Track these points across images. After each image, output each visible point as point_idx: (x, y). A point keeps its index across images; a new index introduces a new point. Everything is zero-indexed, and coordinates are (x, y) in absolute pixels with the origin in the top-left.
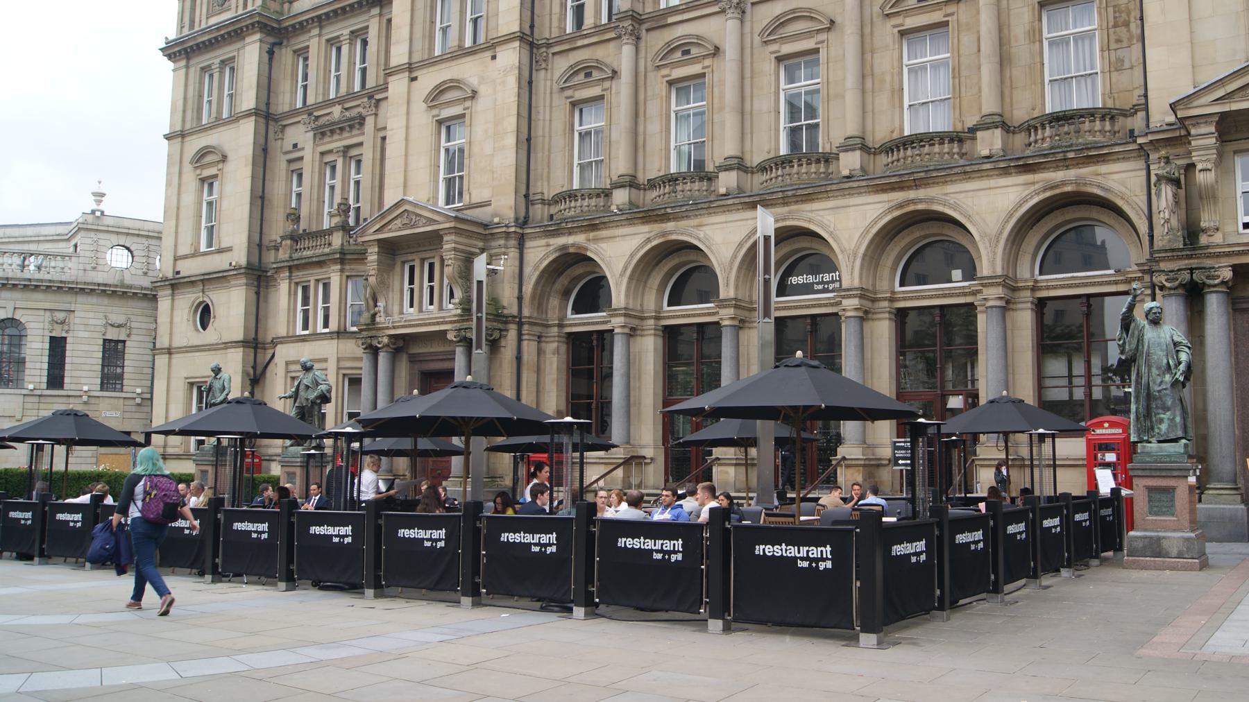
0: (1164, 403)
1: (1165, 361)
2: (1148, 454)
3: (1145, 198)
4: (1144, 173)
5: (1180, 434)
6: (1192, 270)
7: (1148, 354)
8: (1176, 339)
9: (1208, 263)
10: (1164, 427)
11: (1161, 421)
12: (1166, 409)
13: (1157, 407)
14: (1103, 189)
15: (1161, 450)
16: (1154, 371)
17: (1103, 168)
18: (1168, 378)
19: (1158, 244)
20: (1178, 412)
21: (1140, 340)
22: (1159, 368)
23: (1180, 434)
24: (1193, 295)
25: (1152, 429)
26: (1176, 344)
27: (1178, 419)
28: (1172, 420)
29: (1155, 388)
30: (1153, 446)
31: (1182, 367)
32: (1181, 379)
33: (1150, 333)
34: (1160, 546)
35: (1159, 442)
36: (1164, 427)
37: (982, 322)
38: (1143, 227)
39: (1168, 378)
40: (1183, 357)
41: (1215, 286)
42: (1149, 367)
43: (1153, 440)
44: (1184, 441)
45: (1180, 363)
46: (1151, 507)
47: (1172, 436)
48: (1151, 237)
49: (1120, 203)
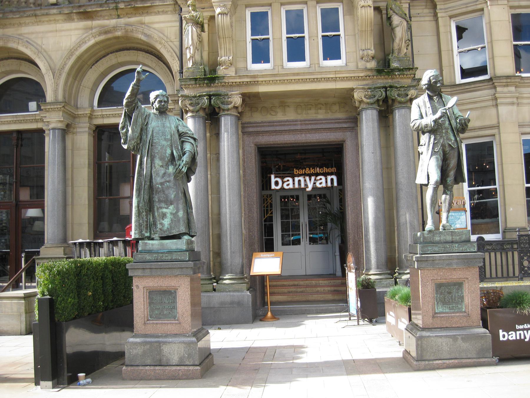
0: (167, 196)
1: (169, 151)
2: (150, 252)
3: (178, 44)
4: (178, 24)
5: (183, 229)
6: (210, 96)
7: (151, 144)
8: (181, 129)
9: (222, 90)
10: (166, 222)
11: (164, 216)
12: (169, 202)
13: (160, 201)
14: (146, 35)
15: (162, 245)
16: (158, 162)
17: (147, 19)
18: (171, 169)
19: (185, 75)
20: (181, 206)
21: (143, 129)
22: (161, 159)
23: (183, 229)
24: (211, 116)
25: (155, 224)
26: (181, 135)
27: (181, 214)
28: (175, 215)
29: (157, 180)
30: (155, 244)
31: (185, 158)
32: (185, 170)
33: (154, 124)
34: (160, 352)
35: (162, 238)
36: (166, 222)
37: (49, 141)
38: (175, 66)
39: (171, 169)
40: (188, 147)
41: (228, 110)
42: (152, 159)
43: (156, 236)
44: (186, 237)
45: (184, 154)
46: (152, 310)
47: (175, 232)
48: (181, 72)
49: (159, 47)
